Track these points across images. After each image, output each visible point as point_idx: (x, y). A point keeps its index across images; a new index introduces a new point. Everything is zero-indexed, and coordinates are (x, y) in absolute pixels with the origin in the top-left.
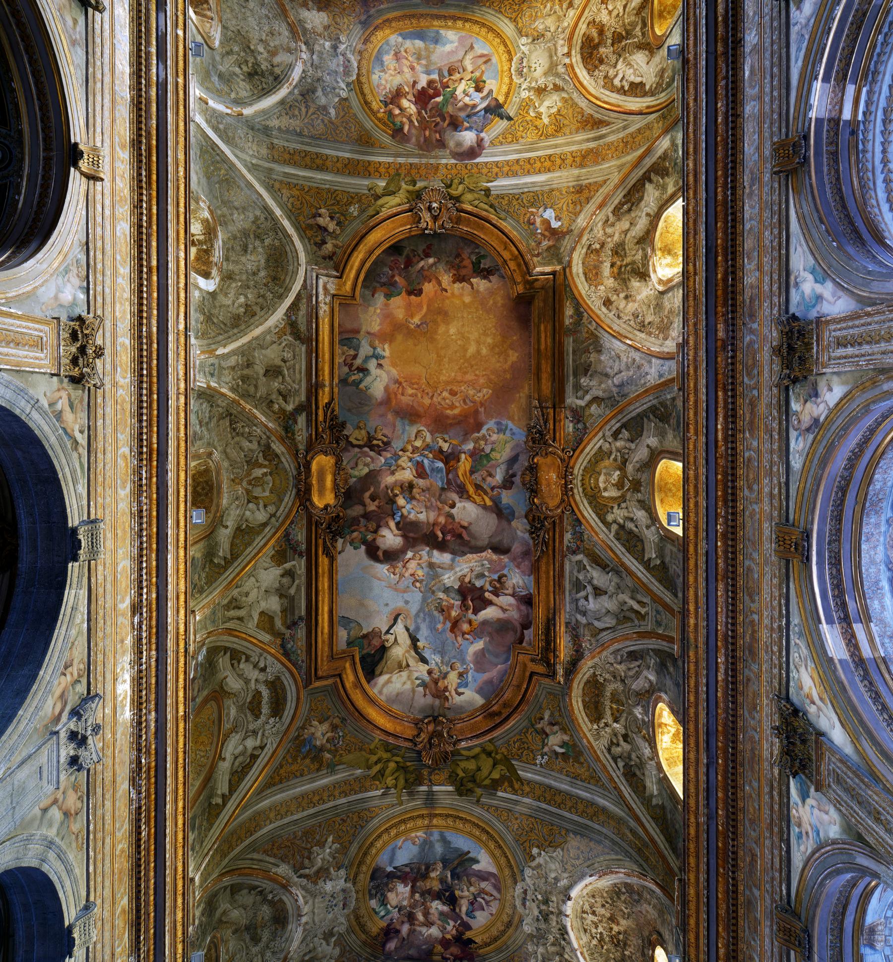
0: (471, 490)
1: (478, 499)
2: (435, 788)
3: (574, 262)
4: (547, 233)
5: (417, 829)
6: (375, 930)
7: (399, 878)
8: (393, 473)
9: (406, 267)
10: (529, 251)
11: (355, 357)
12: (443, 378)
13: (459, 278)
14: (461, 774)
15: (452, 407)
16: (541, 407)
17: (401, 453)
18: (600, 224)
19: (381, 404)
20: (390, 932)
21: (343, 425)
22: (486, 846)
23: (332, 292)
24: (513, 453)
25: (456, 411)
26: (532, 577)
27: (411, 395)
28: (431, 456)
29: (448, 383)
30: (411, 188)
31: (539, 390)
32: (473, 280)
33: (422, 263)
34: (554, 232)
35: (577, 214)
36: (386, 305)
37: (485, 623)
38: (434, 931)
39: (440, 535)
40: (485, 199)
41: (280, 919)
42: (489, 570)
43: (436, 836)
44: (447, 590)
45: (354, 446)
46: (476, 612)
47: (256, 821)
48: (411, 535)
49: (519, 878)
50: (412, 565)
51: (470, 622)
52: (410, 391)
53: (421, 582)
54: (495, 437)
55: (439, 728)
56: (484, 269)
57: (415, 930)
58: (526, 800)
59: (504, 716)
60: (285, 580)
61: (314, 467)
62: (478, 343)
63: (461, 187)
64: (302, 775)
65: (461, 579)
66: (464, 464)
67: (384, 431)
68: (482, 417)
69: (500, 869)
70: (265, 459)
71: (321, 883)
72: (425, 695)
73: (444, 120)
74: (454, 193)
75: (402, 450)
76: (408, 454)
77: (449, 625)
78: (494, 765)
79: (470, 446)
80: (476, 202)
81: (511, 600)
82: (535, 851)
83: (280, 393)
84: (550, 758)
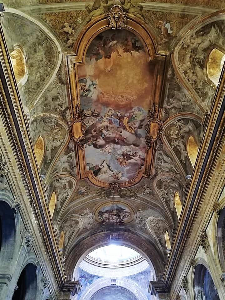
0: (128, 128)
1: (130, 131)
2: (114, 197)
3: (175, 52)
4: (166, 35)
5: (110, 204)
6: (100, 221)
7: (106, 213)
8: (101, 123)
9: (104, 45)
10: (157, 42)
11: (85, 86)
12: (119, 91)
13: (127, 50)
14: (121, 194)
15: (122, 101)
16: (154, 106)
17: (104, 117)
19: (95, 102)
20: (103, 221)
21: (83, 111)
22: (128, 208)
23: (74, 62)
24: (143, 118)
25: (123, 103)
26: (145, 154)
27: (107, 98)
28: (114, 117)
29: (120, 93)
30: (105, 5)
33: (111, 43)
34: (169, 35)
35: (180, 29)
36: (96, 63)
37: (130, 163)
38: (114, 221)
39: (117, 140)
40: (140, 12)
41: (77, 223)
42: (132, 150)
43: (115, 205)
44: (119, 155)
45: (87, 117)
46: (127, 160)
47: (69, 210)
48: (108, 141)
49: (135, 213)
50: (108, 149)
51: (126, 162)
52: (106, 96)
53: (111, 152)
54: (137, 112)
55: (116, 186)
57: (109, 221)
58: (139, 200)
59: (134, 184)
60: (69, 158)
61: (74, 127)
62: (133, 78)
63: (129, 4)
64: (79, 198)
65: (123, 152)
66: (126, 120)
67: (97, 110)
68: (133, 105)
69: (131, 211)
71: (86, 216)
72: (112, 178)
74: (126, 7)
75: (104, 116)
76: (106, 117)
77: (119, 163)
78: (131, 193)
79: (128, 114)
80: (136, 13)
81: (139, 159)
82: (140, 210)
83: (59, 105)
84: (146, 194)
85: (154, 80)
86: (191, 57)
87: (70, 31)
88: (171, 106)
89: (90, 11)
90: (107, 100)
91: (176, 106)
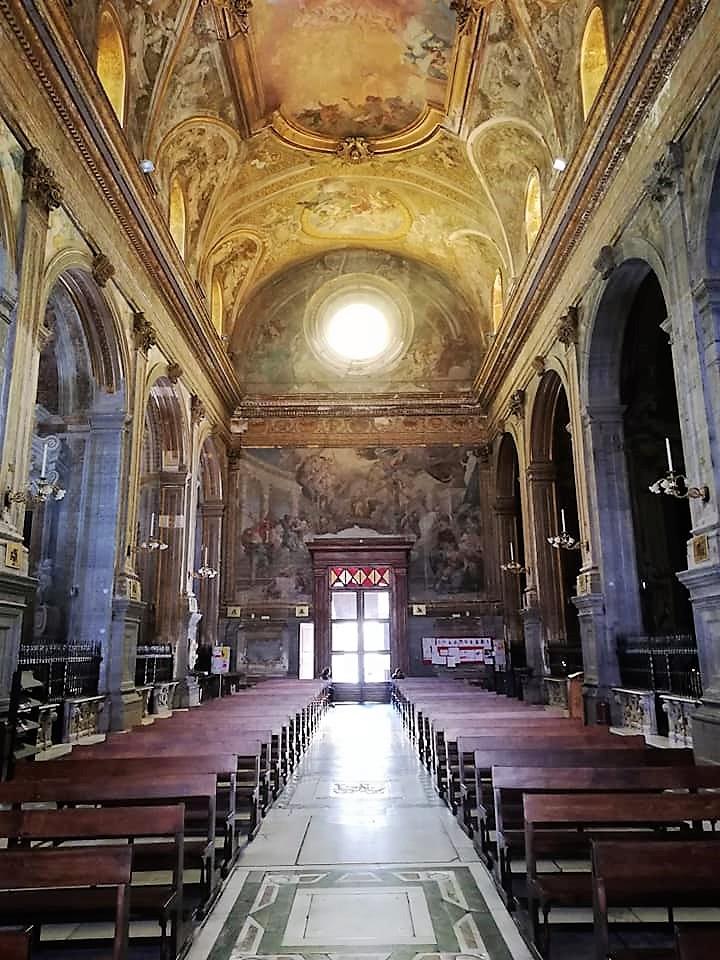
10: (272, 139)
11: (434, 61)
18: (221, 175)
19: (412, 14)
27: (378, 18)
31: (246, 45)
32: (320, 108)
56: (310, 116)
70: (540, 8)
73: (349, 197)
85: (259, 80)
86: (205, 154)
87: (442, 155)
88: (199, 57)
89: (404, 161)
90: (380, 10)
91: (188, 67)
